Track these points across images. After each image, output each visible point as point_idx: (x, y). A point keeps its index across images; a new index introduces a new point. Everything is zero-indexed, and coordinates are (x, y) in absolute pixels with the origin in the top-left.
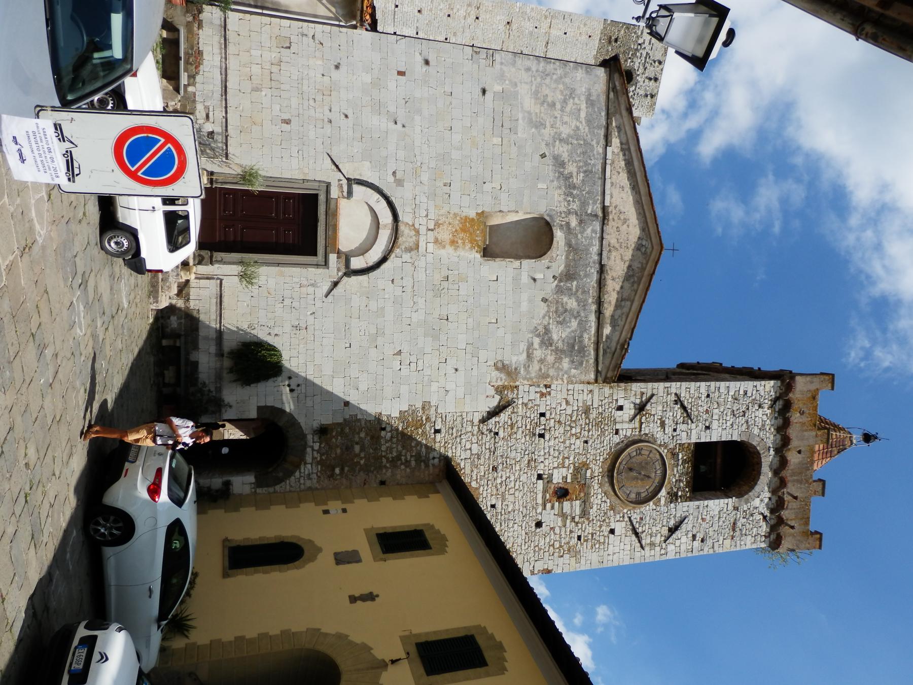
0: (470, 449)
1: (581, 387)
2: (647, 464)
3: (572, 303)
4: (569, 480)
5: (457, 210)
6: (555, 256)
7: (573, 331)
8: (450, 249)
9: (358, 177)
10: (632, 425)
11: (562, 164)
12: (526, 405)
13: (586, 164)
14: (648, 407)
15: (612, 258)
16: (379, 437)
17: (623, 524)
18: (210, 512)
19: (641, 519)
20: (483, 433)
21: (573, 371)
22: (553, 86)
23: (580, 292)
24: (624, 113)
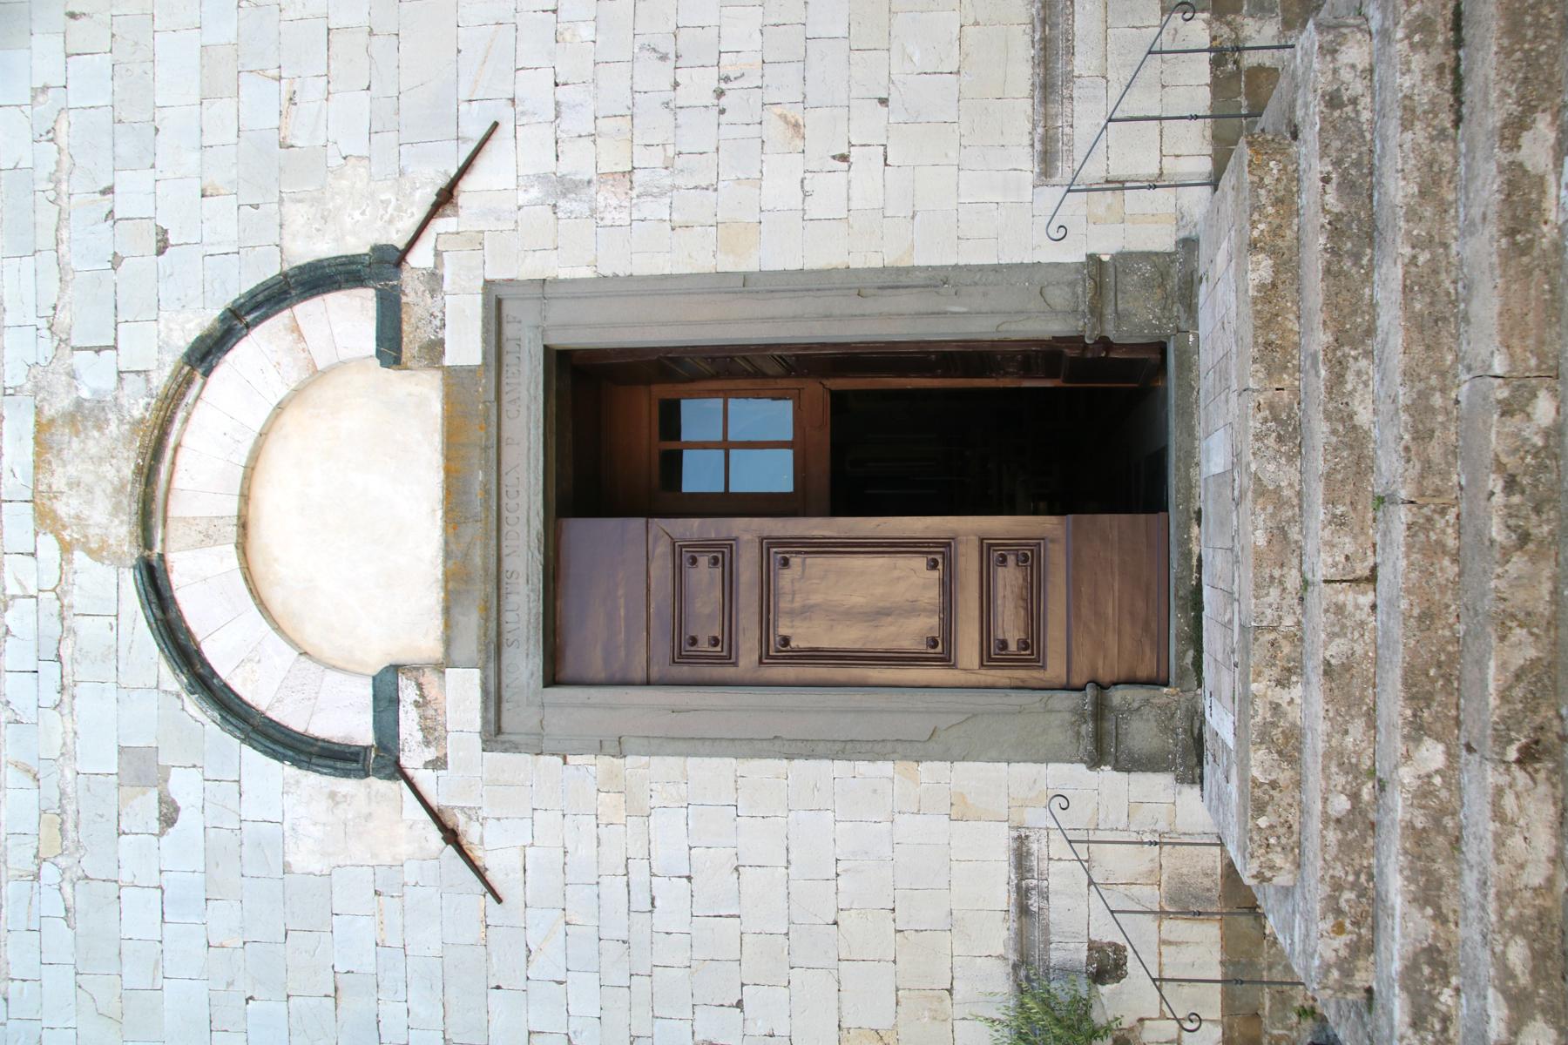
9: (347, 786)
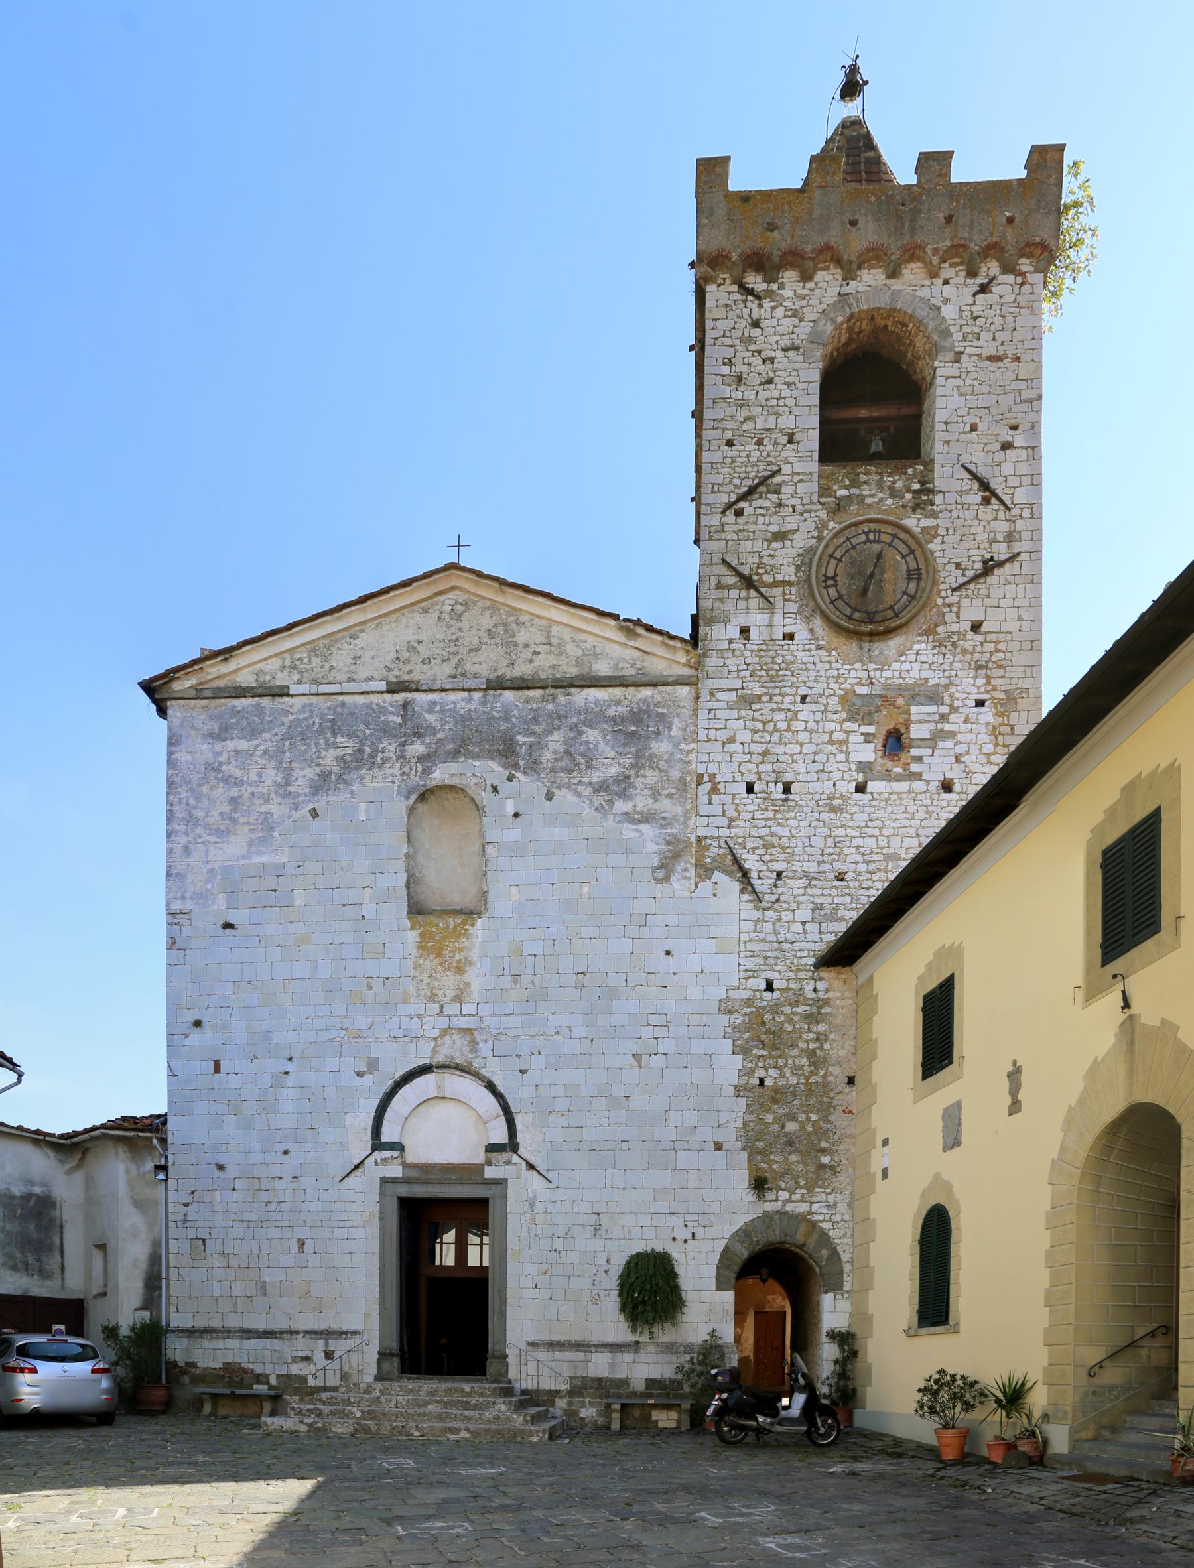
0: (804, 923)
1: (703, 714)
2: (852, 564)
3: (556, 741)
4: (871, 729)
5: (409, 963)
6: (475, 780)
7: (604, 738)
8: (471, 974)
10: (779, 602)
11: (324, 776)
12: (732, 820)
13: (321, 732)
14: (745, 570)
15: (475, 668)
16: (776, 1090)
17: (965, 602)
18: (869, 1360)
19: (958, 566)
20: (778, 900)
21: (675, 732)
22: (206, 803)
23: (536, 728)
24: (232, 665)
